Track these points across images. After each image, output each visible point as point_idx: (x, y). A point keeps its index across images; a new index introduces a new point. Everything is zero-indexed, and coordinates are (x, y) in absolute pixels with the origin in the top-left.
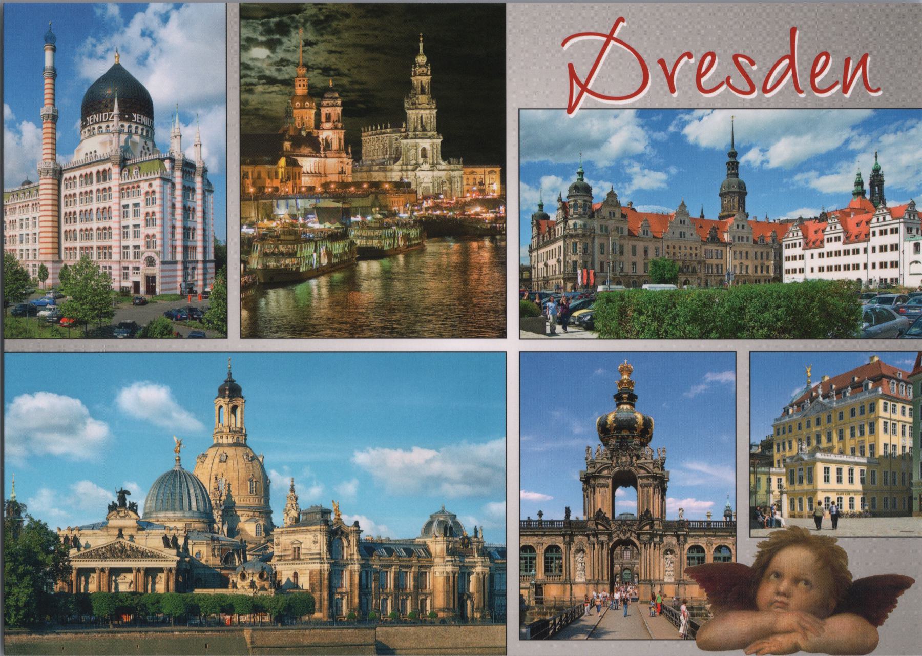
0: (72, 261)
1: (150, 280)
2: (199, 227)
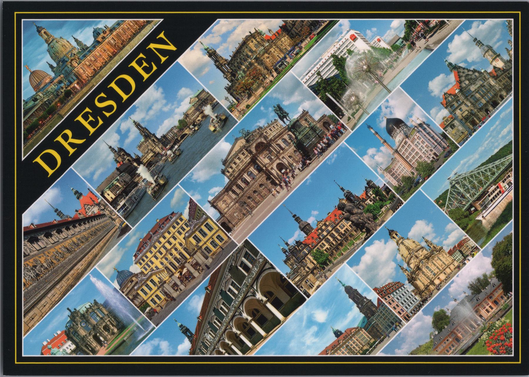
0: (416, 165)
1: (435, 154)
2: (434, 134)
